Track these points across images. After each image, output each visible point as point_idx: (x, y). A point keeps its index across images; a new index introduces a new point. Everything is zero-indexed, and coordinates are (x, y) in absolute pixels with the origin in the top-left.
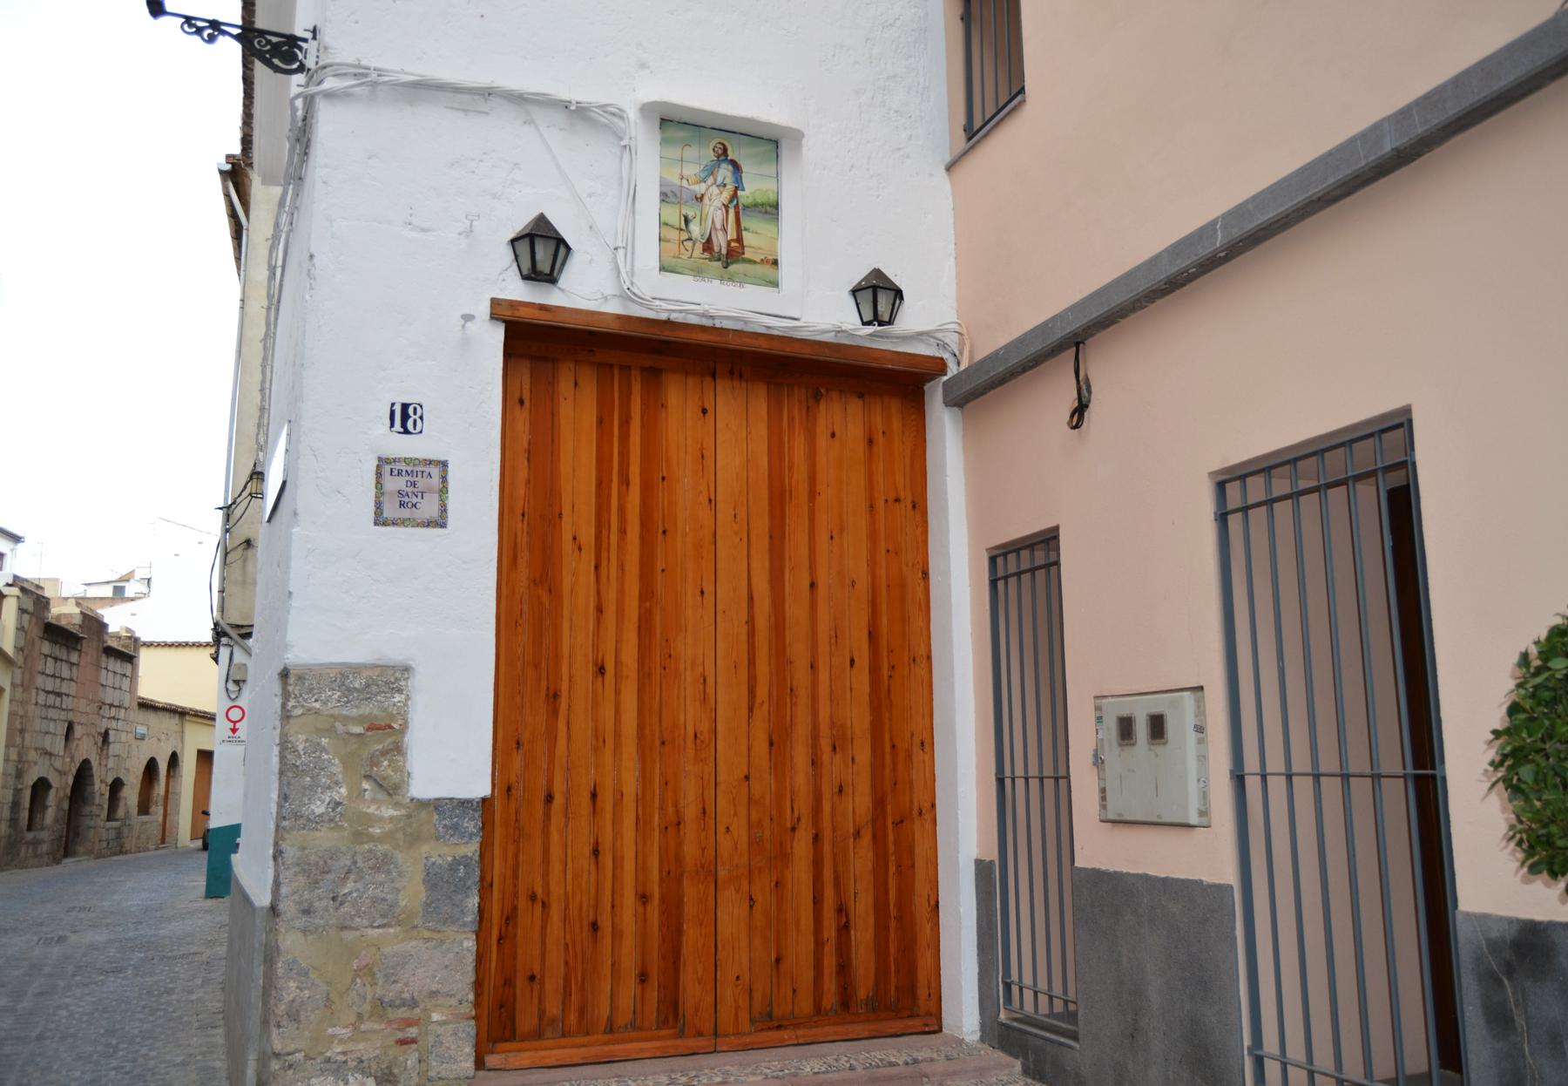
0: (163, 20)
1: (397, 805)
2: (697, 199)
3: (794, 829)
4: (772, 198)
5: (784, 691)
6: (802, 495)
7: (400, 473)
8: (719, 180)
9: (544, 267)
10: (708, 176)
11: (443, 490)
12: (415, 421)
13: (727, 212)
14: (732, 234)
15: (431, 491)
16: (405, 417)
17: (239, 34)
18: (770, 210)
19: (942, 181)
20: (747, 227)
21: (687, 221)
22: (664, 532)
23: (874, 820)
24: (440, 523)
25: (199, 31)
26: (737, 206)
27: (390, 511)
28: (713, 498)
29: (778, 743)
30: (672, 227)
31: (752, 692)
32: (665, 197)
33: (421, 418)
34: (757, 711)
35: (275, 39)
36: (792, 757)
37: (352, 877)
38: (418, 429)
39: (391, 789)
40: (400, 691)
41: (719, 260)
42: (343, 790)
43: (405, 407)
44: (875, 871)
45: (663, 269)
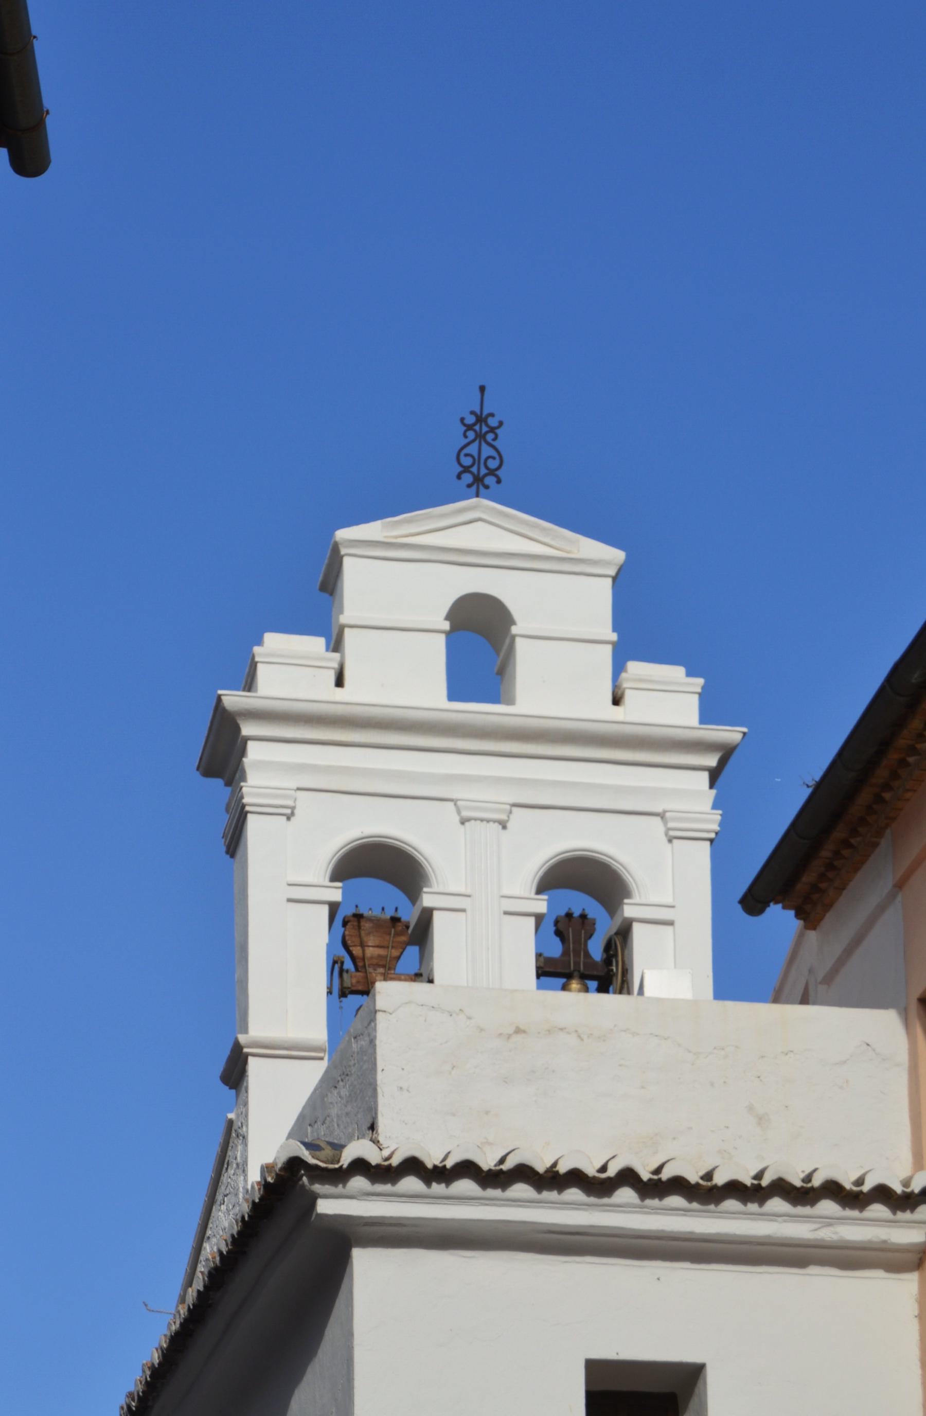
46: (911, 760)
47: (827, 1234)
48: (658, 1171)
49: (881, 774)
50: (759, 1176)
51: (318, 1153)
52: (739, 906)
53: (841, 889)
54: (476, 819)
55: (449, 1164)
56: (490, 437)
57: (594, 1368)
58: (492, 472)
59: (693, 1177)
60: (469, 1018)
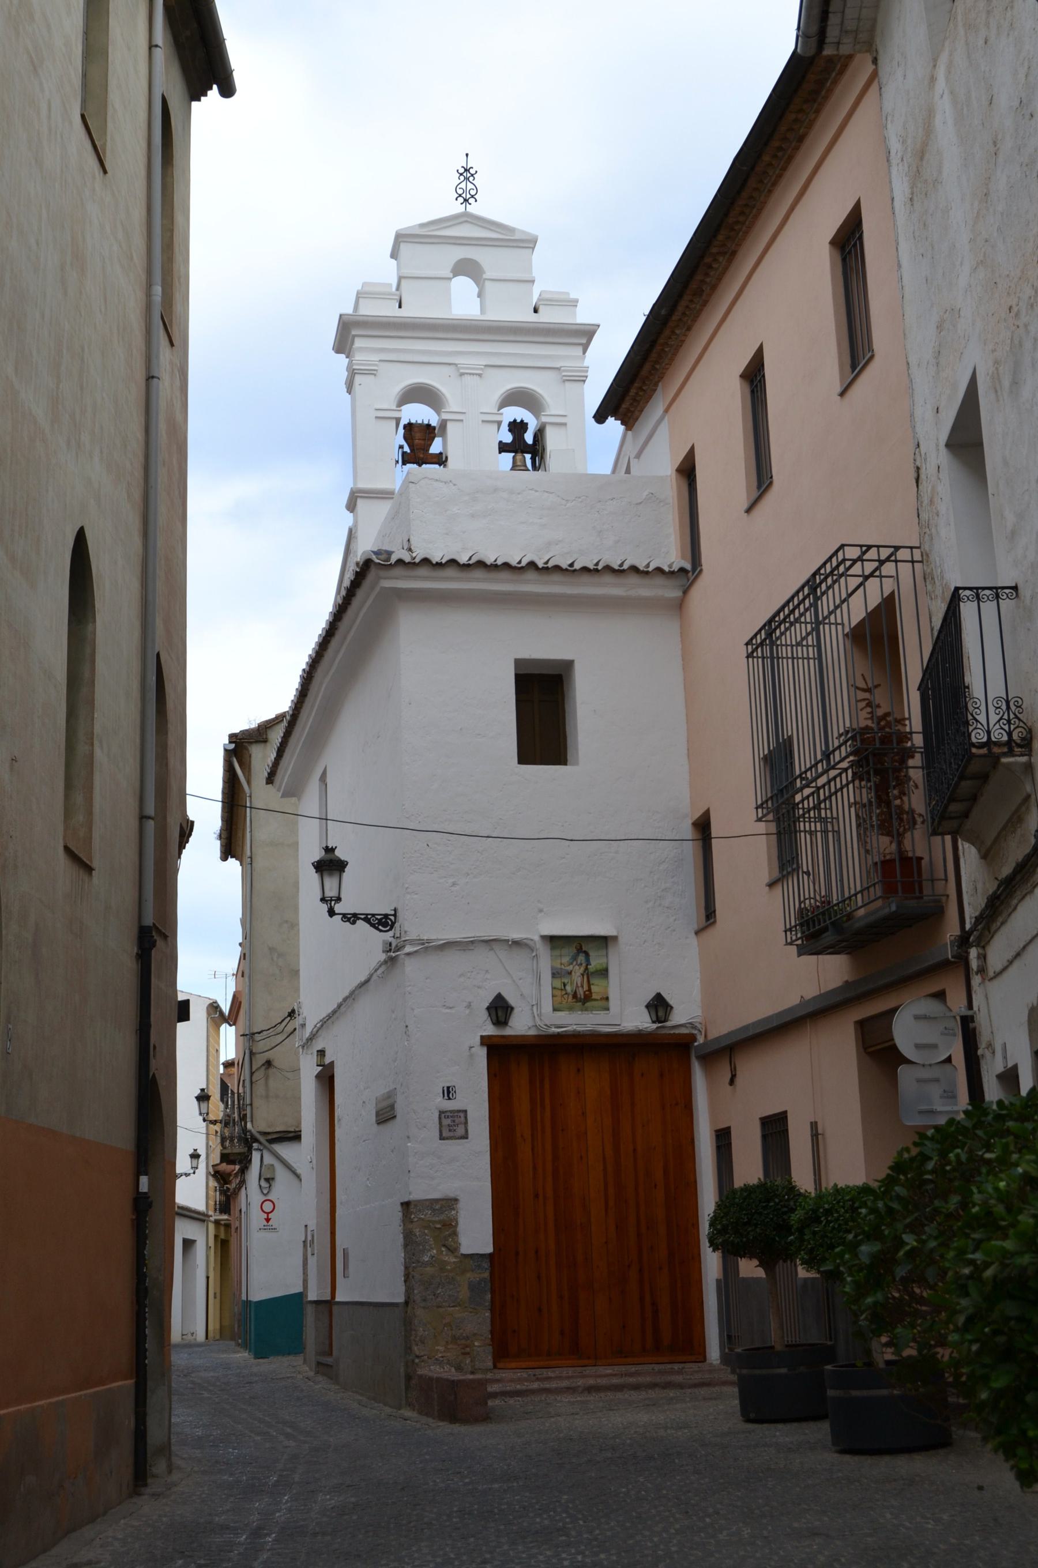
1: (456, 1257)
3: (629, 1266)
4: (605, 966)
7: (448, 1117)
8: (579, 962)
9: (502, 1019)
10: (573, 961)
11: (466, 1123)
14: (586, 987)
15: (461, 1123)
16: (448, 1092)
18: (604, 973)
24: (465, 1137)
25: (349, 920)
26: (588, 974)
27: (445, 1134)
30: (558, 989)
32: (554, 975)
35: (379, 917)
37: (441, 1287)
39: (453, 1250)
40: (454, 1209)
41: (580, 1001)
42: (435, 1251)
43: (448, 1088)
46: (667, 349)
47: (633, 593)
48: (547, 563)
49: (654, 355)
50: (597, 564)
56: (471, 179)
57: (518, 663)
58: (472, 196)
59: (564, 565)
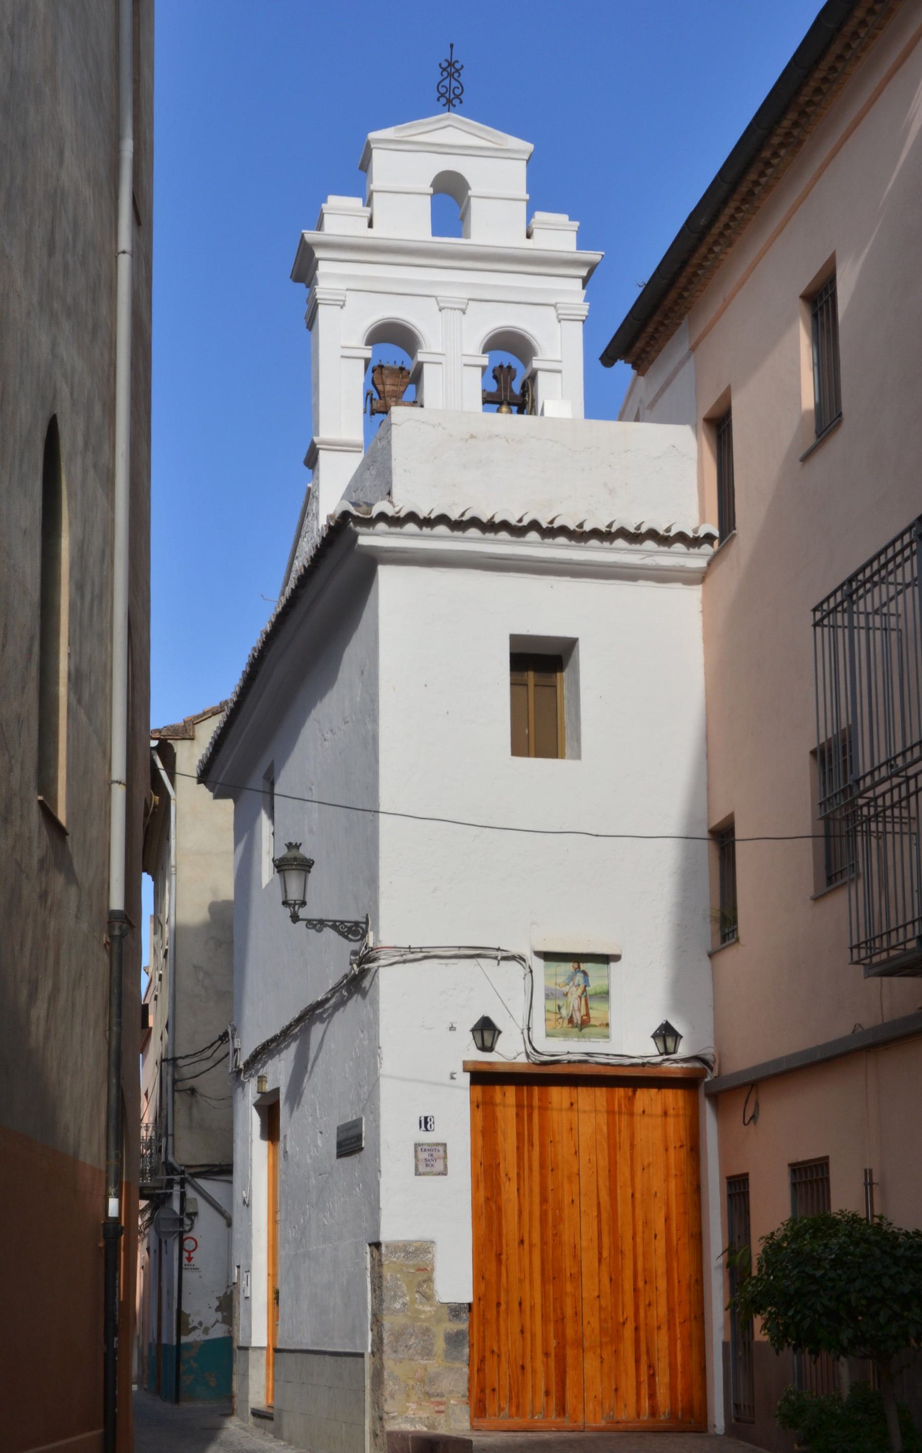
0: (299, 923)
1: (431, 1305)
2: (564, 995)
3: (624, 1324)
4: (605, 988)
5: (617, 1250)
6: (626, 1146)
7: (425, 1150)
8: (576, 983)
9: (488, 1043)
10: (569, 982)
11: (445, 1158)
12: (431, 1125)
13: (581, 1000)
14: (583, 1012)
15: (439, 1158)
16: (426, 1123)
17: (332, 925)
18: (604, 995)
19: (706, 961)
20: (592, 1006)
21: (559, 1008)
22: (552, 1170)
23: (669, 1322)
24: (444, 1173)
25: (314, 927)
26: (586, 997)
27: (422, 1169)
28: (577, 1149)
29: (615, 1282)
30: (551, 1012)
31: (600, 1253)
32: (547, 997)
33: (433, 1123)
34: (603, 1262)
35: (349, 925)
36: (622, 1286)
37: (413, 1337)
38: (432, 1129)
39: (428, 1297)
40: (430, 1253)
41: (577, 1027)
42: (408, 1298)
43: (426, 1118)
44: (669, 1346)
45: (548, 1035)
46: (700, 272)
47: (649, 561)
48: (552, 522)
49: (682, 280)
50: (610, 526)
51: (359, 509)
52: (600, 362)
53: (659, 351)
54: (448, 308)
55: (433, 516)
56: (456, 75)
57: (515, 640)
58: (457, 97)
59: (572, 526)
60: (444, 429)
